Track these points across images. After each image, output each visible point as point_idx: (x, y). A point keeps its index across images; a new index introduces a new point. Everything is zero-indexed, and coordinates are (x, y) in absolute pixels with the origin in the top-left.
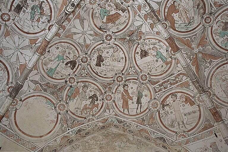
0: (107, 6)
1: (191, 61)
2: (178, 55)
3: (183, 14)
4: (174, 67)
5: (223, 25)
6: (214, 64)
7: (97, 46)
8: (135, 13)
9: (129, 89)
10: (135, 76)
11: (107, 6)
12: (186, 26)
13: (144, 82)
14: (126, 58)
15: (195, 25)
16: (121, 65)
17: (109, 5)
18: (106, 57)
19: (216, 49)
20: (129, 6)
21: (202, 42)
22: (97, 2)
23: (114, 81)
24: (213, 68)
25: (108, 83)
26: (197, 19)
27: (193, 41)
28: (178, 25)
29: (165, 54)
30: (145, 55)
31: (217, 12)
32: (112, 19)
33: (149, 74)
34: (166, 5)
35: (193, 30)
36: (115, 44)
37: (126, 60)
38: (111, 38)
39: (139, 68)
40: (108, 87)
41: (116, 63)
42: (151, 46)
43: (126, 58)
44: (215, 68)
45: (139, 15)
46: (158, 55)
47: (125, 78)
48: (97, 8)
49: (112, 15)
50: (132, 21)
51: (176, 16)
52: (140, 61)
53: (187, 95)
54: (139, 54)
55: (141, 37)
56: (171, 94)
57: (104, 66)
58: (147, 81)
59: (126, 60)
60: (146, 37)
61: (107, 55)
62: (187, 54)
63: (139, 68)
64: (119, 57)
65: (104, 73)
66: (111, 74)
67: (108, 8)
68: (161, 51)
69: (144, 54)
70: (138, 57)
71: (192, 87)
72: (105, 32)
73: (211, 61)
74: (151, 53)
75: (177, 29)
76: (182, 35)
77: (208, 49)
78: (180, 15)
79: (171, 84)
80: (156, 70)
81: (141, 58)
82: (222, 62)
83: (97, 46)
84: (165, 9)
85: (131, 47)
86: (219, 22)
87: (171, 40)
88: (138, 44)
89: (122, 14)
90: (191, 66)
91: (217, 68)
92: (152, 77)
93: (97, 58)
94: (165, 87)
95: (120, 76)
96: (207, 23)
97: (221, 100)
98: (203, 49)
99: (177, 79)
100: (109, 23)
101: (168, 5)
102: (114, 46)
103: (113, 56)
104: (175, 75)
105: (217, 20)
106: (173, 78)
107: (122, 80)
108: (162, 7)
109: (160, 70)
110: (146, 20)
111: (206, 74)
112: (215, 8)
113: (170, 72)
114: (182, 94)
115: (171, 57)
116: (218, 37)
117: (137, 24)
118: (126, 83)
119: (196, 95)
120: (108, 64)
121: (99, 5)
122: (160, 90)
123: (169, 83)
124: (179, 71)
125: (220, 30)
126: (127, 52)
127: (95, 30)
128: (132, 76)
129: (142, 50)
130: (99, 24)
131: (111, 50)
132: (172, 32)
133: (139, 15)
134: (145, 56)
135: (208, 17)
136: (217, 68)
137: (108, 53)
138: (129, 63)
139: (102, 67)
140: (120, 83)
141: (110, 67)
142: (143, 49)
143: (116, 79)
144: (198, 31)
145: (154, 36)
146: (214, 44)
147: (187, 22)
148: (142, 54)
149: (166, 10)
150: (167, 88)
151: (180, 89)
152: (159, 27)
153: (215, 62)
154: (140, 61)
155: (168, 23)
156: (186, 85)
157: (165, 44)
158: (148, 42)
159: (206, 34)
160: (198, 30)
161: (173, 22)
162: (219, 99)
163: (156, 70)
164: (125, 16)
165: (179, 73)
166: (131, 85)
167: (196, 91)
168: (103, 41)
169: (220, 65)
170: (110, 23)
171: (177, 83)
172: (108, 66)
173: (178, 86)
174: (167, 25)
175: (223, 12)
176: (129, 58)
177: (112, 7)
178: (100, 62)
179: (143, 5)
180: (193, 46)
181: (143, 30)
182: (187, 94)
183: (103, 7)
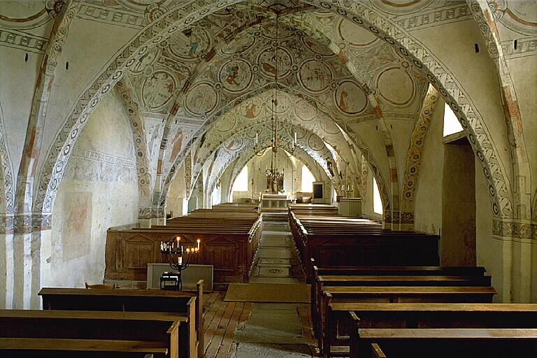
29: (198, 50)
46: (194, 46)
71: (183, 82)
92: (169, 49)
109: (179, 52)
115: (198, 56)
122: (162, 63)
134: (187, 34)
167: (182, 86)
181: (213, 27)
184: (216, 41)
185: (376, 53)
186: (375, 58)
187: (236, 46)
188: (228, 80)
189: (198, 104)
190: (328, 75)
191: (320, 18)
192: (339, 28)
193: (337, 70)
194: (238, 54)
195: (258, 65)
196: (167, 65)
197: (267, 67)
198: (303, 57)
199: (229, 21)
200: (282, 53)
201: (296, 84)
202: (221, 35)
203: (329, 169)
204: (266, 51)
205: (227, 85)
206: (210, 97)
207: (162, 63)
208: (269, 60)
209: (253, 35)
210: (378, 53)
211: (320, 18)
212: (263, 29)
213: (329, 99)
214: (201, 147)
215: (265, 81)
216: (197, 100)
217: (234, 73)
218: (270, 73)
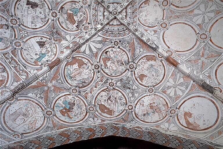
0: (81, 13)
1: (41, 80)
2: (45, 68)
3: (78, 71)
4: (33, 67)
5: (72, 102)
6: (40, 100)
7: (47, 3)
8: (77, 35)
9: (4, 29)
10: (18, 37)
11: (81, 13)
12: (69, 74)
13: (14, 44)
14: (36, 29)
15: (69, 81)
16: (29, 25)
17: (81, 16)
18: (36, 11)
19: (53, 100)
20: (81, 30)
21: (58, 89)
22: (84, 5)
23: (12, 16)
24: (36, 100)
25: (9, 10)
26: (75, 83)
27: (57, 81)
28: (69, 68)
30: (40, 45)
31: (81, 96)
32: (70, 18)
33: (22, 48)
34: (84, 58)
35: (66, 81)
36: (48, 20)
37: (33, 29)
38: (54, 17)
39: (27, 40)
40: (5, 9)
41: (30, 19)
43: (36, 29)
44: (36, 102)
45: (75, 38)
46: (43, 55)
47: (16, 27)
48: (80, 6)
49: (73, 18)
50: (69, 33)
51: (76, 66)
52: (33, 42)
53: (6, 81)
54: (41, 40)
55: (56, 41)
56: (4, 67)
57: (27, 8)
58: (15, 47)
59: (33, 29)
60: (57, 45)
61: (38, 12)
62: (46, 77)
63: (27, 40)
64: (37, 23)
65: (19, 7)
66: (19, 14)
67: (79, 15)
68: (47, 57)
69: (42, 44)
70: (38, 39)
71: (16, 84)
72: (59, 12)
73: (42, 98)
74: (44, 49)
75: (66, 67)
76: (62, 71)
77: (52, 95)
78: (77, 69)
79: (15, 67)
80: (27, 54)
81: (37, 42)
82: (43, 106)
83: (47, 3)
84: (81, 57)
85: (47, 33)
86: (74, 99)
87: (58, 62)
88: (50, 39)
89: (74, 26)
90: (36, 81)
91: (36, 103)
92: (19, 51)
93: (35, 3)
94: (10, 62)
95: (17, 23)
96: (72, 91)
97: (6, 110)
98: (51, 91)
99: (21, 72)
100: (67, 15)
101: (83, 60)
102: (47, 19)
103: (38, 17)
104: (25, 69)
105: (75, 97)
106: (21, 68)
107: (13, 24)
108: (82, 54)
109: (28, 57)
110: (71, 43)
111: (30, 95)
112: (83, 94)
113: (28, 66)
114: (7, 77)
115: (42, 64)
116: (63, 100)
117: (68, 37)
118: (10, 27)
119: (7, 88)
120: (29, 12)
121: (82, 7)
122: (7, 58)
123: (16, 65)
124: (30, 72)
125: (69, 100)
126: (42, 30)
127: (61, 3)
128: (18, 33)
129: (45, 42)
130: (66, 7)
131: (43, 17)
132: (64, 64)
133: (75, 38)
134: (40, 45)
135: (77, 91)
136: (36, 103)
137: (41, 13)
138: (32, 31)
139: (25, 6)
140: (10, 22)
141: (26, 13)
142: (45, 43)
143: (14, 18)
144: (66, 85)
145: (59, 50)
146: (57, 98)
147: (71, 75)
148: (41, 42)
149: (80, 58)
150: (10, 64)
151: (11, 74)
152: (67, 52)
153: (42, 101)
154: (33, 42)
155: (70, 60)
156: (16, 79)
157: (54, 58)
158: (53, 46)
159: (64, 91)
160: (66, 84)
161: (71, 64)
162: (7, 108)
163: (27, 54)
164: (73, 28)
165: (29, 72)
166: (8, 32)
168: (51, 9)
169: (40, 105)
170: (67, 16)
171: (18, 72)
172: (27, 12)
173: (14, 72)
174: (69, 59)
175: (82, 100)
176: (36, 31)
177: (80, 18)
178: (31, 4)
179: (84, 38)
180: (54, 82)
182: (7, 81)
183: (80, 10)
185: (201, 55)
186: (203, 59)
188: (61, 111)
189: (19, 121)
191: (147, 30)
192: (163, 39)
193: (171, 95)
195: (95, 105)
196: (10, 62)
197: (103, 108)
198: (136, 95)
199: (77, 35)
201: (132, 120)
205: (59, 114)
206: (36, 120)
207: (7, 58)
208: (105, 101)
209: (93, 66)
210: (203, 54)
211: (147, 30)
212: (102, 62)
213: (173, 125)
215: (100, 121)
216: (20, 117)
217: (70, 108)
218: (105, 115)
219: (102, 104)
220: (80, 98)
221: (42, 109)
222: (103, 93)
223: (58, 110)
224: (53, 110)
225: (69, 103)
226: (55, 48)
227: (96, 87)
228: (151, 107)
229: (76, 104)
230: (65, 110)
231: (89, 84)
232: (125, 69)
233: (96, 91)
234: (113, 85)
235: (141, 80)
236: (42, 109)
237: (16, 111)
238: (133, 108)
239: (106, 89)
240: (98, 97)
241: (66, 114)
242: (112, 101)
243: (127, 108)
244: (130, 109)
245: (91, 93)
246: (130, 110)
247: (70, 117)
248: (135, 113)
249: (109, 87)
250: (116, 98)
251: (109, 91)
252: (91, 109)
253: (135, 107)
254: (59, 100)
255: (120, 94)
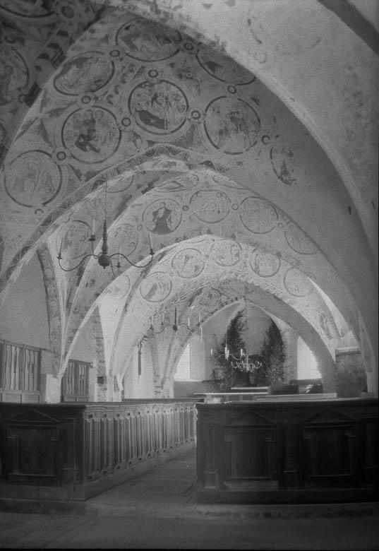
5: (90, 118)
8: (53, 26)
42: (8, 63)
45: (50, 33)
133: (50, 33)
184: (38, 68)
187: (84, 81)
190: (254, 123)
194: (89, 94)
197: (146, 117)
200: (168, 89)
202: (44, 56)
203: (322, 327)
204: (140, 86)
205: (77, 151)
206: (50, 177)
212: (123, 44)
214: (78, 285)
217: (89, 131)
219: (143, 111)
220: (100, 107)
221: (49, 155)
222: (140, 90)
223: (71, 144)
224: (66, 148)
225: (85, 123)
226: (19, 58)
227: (124, 82)
228: (233, 119)
229: (97, 120)
230: (82, 140)
231: (108, 82)
232: (174, 50)
233: (125, 91)
234: (157, 74)
235: (213, 69)
236: (49, 155)
237: (17, 178)
238: (202, 116)
239: (145, 83)
240: (132, 97)
241: (87, 147)
242: (160, 104)
243: (190, 117)
244: (195, 118)
245: (117, 93)
246: (196, 121)
247: (96, 151)
248: (205, 125)
249: (150, 78)
250: (167, 98)
251: (152, 85)
252: (126, 122)
253: (205, 115)
254: (66, 125)
255: (174, 89)
